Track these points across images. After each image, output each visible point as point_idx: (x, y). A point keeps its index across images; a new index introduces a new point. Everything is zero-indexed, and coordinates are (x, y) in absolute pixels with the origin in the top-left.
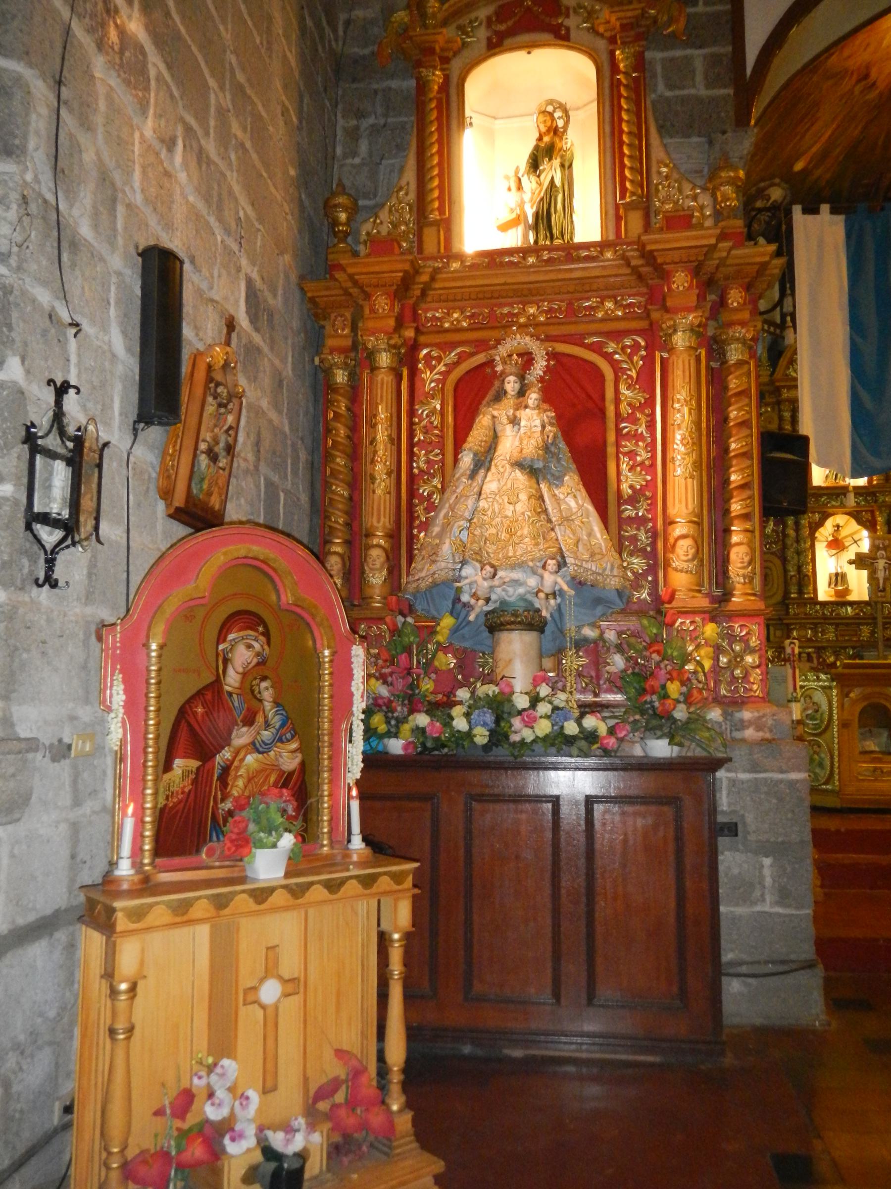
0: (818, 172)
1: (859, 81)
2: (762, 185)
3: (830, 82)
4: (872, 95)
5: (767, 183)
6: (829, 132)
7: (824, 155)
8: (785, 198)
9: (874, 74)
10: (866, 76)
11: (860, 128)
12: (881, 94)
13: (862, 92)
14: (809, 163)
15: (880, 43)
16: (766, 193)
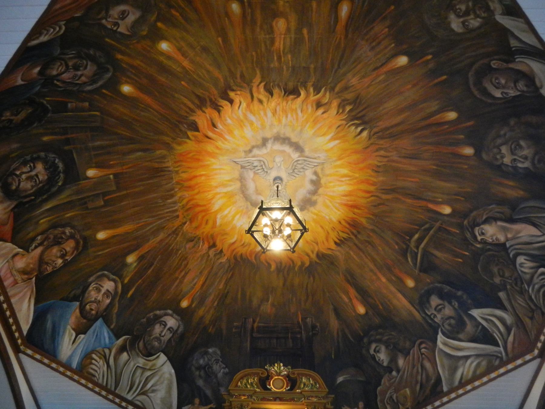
0: (201, 312)
1: (210, 248)
2: (158, 312)
3: (190, 245)
4: (224, 260)
5: (162, 312)
6: (201, 283)
7: (202, 300)
8: (179, 327)
9: (218, 243)
10: (214, 245)
11: (222, 284)
12: (229, 260)
13: (215, 255)
14: (192, 302)
15: (215, 222)
16: (162, 319)
